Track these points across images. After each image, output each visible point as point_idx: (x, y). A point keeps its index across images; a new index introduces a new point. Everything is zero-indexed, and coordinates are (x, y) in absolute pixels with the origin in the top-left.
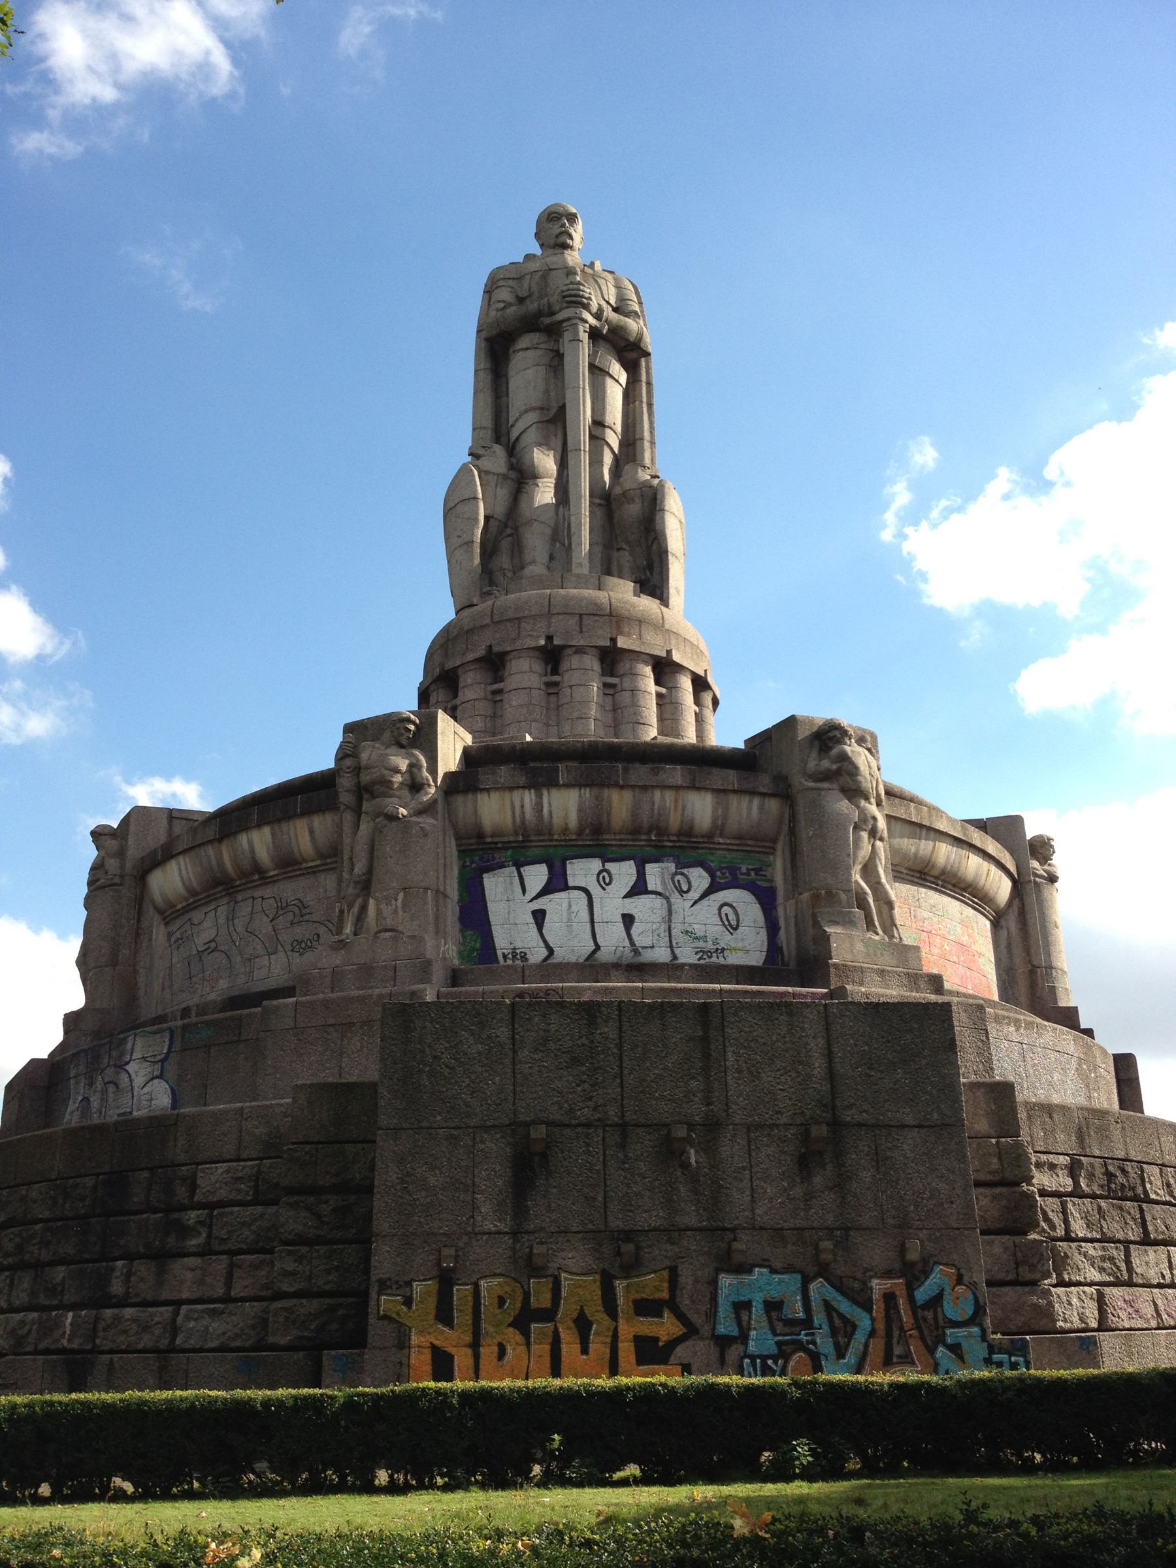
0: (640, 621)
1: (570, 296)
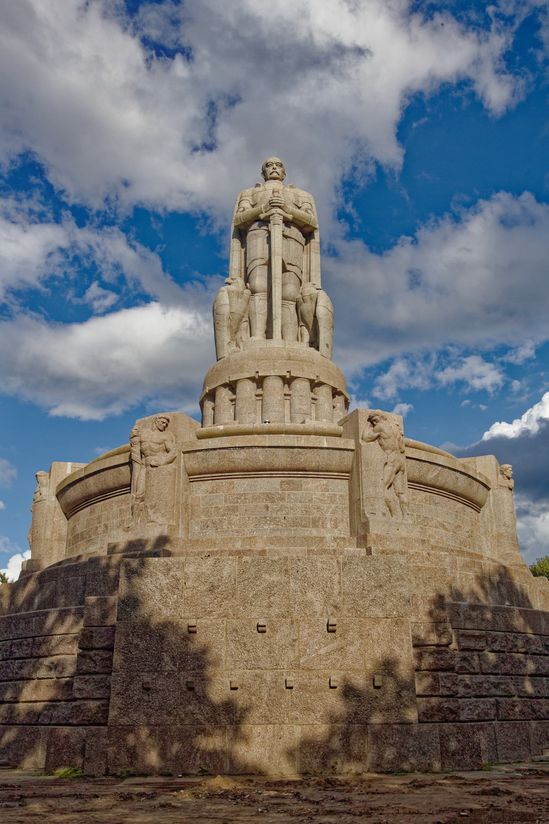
1: (273, 203)
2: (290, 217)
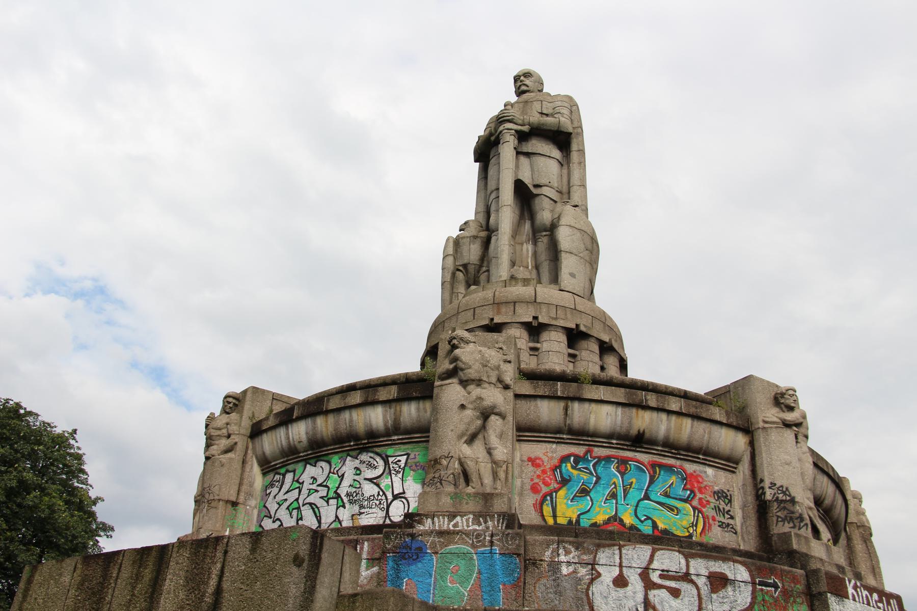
0: (515, 303)
2: (526, 128)
